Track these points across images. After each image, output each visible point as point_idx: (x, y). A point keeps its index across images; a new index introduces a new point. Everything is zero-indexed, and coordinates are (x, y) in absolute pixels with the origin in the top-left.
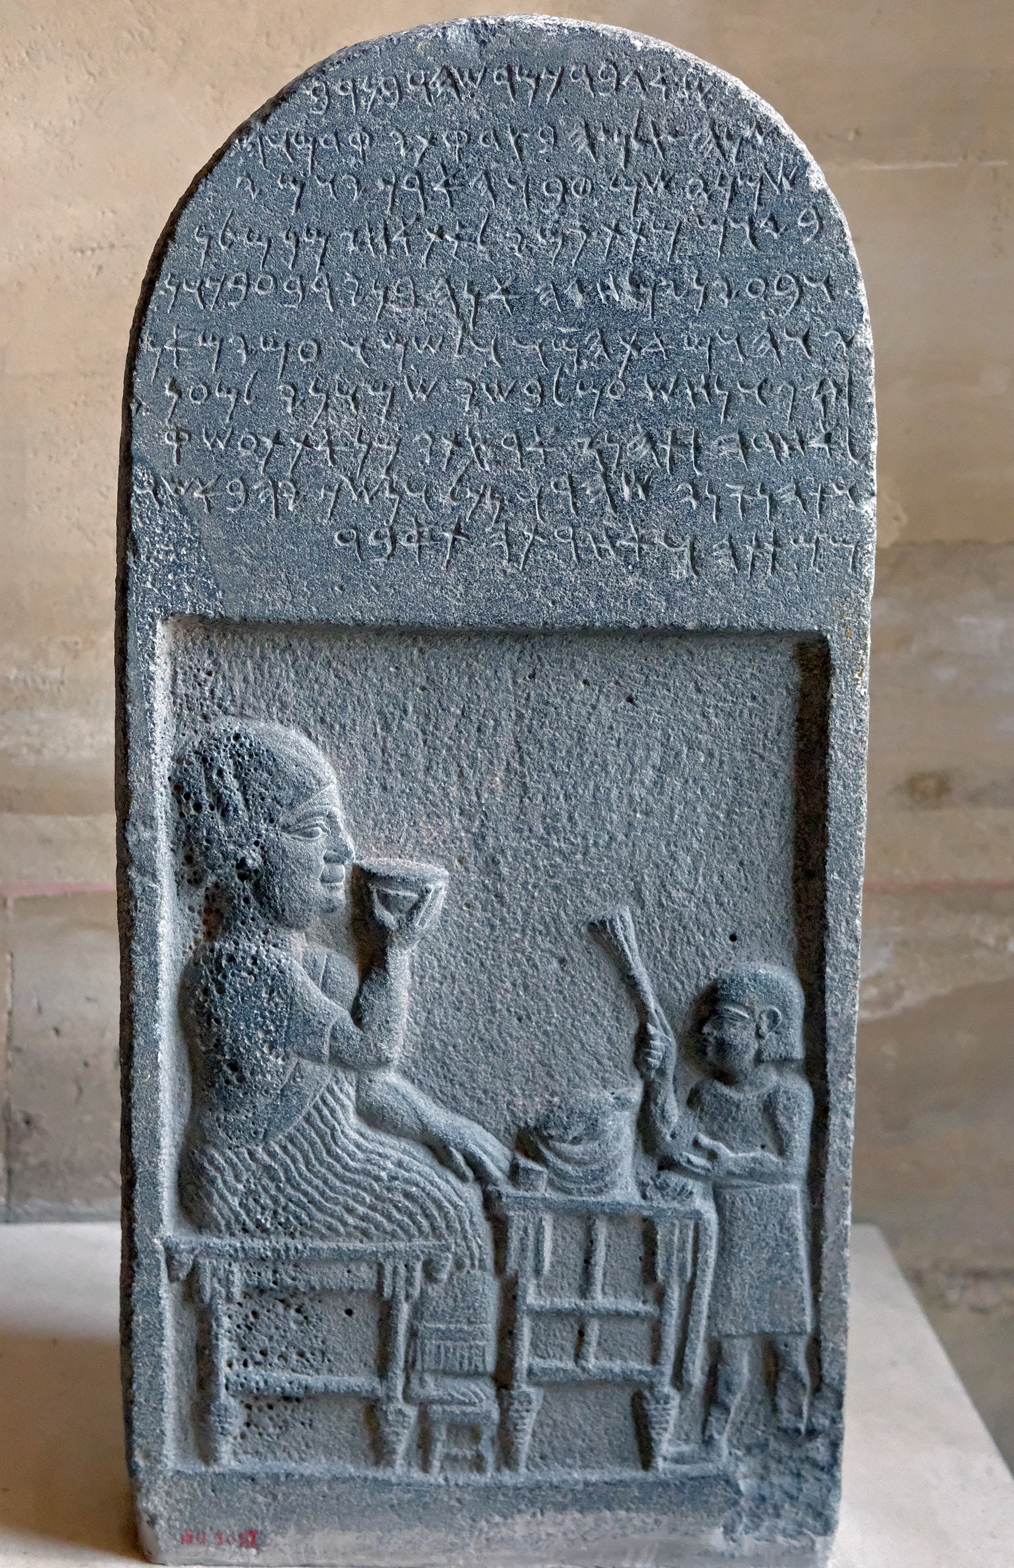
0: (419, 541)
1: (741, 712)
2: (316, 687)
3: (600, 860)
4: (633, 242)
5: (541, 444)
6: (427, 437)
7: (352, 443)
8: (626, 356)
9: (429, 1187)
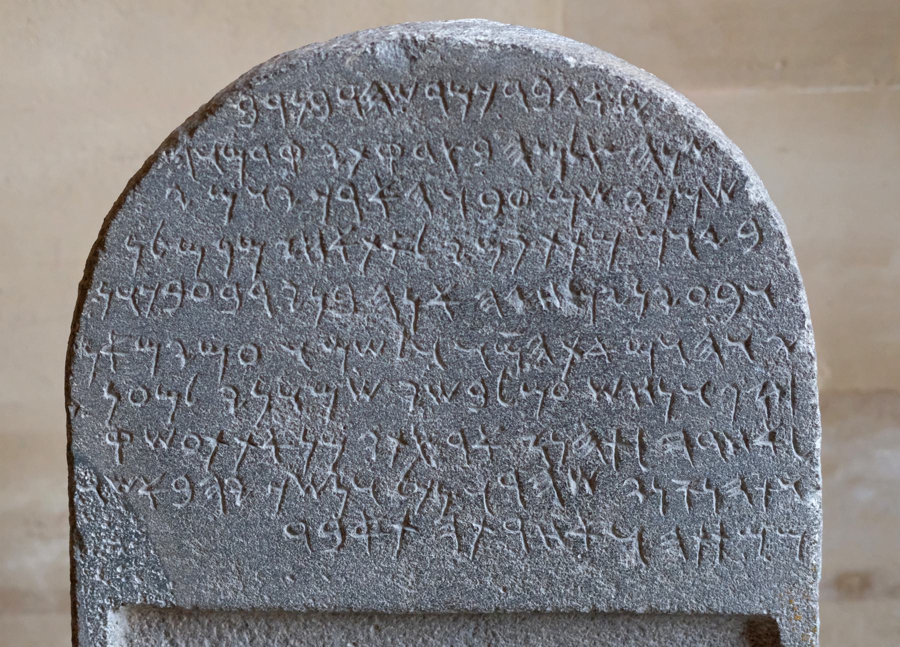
0: (368, 532)
4: (573, 251)
5: (486, 442)
6: (372, 435)
7: (297, 442)
8: (569, 360)
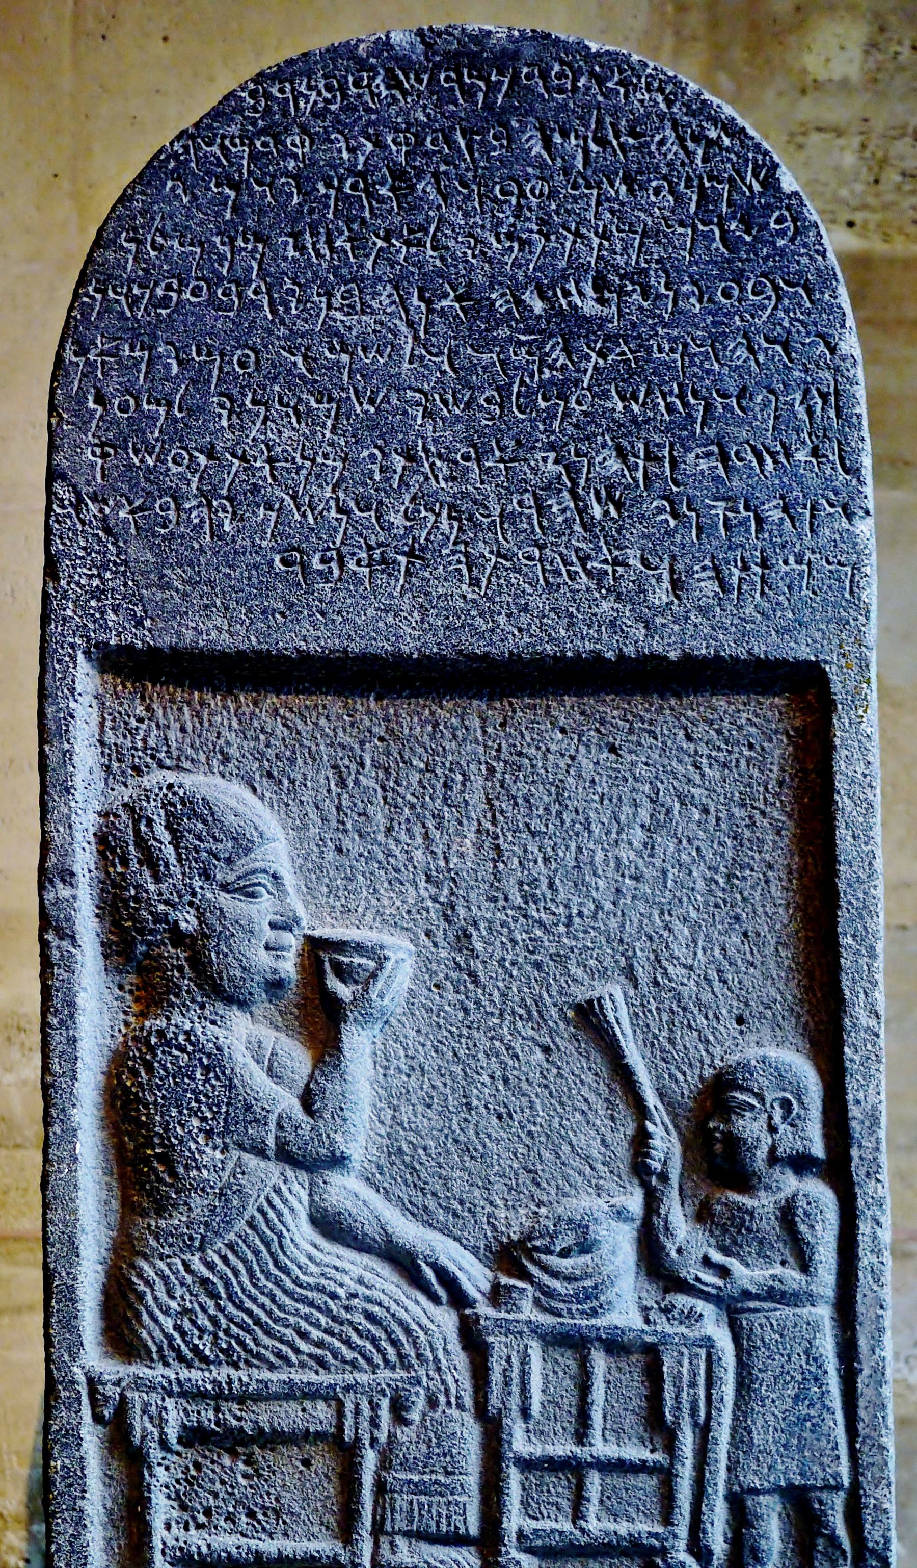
0: (369, 565)
1: (737, 761)
2: (262, 737)
3: (585, 932)
4: (595, 246)
5: (502, 460)
6: (376, 451)
7: (294, 459)
8: (591, 365)
9: (394, 1307)
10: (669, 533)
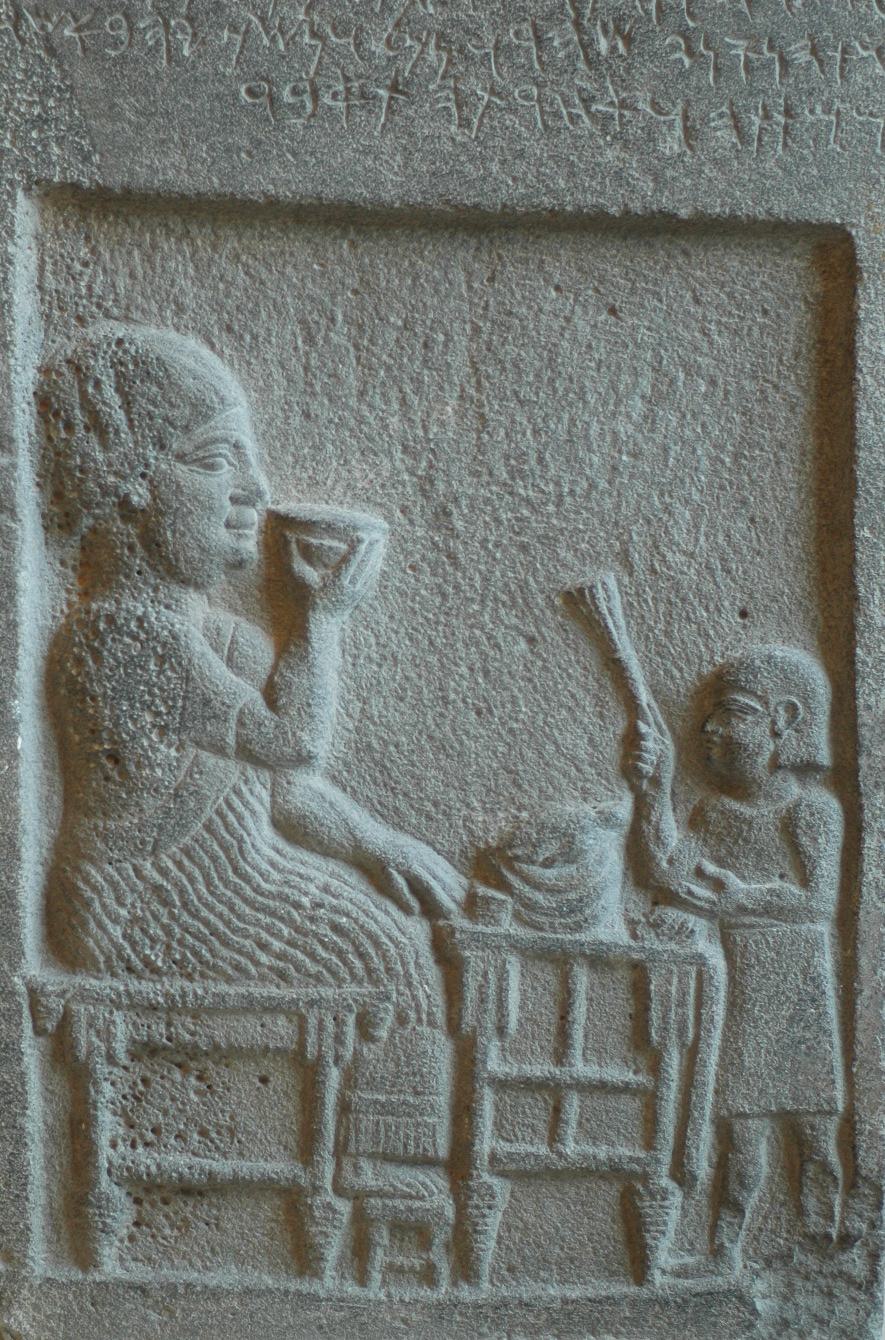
0: (346, 99)
1: (750, 329)
2: (221, 286)
3: (577, 513)
9: (363, 918)
10: (684, 75)
